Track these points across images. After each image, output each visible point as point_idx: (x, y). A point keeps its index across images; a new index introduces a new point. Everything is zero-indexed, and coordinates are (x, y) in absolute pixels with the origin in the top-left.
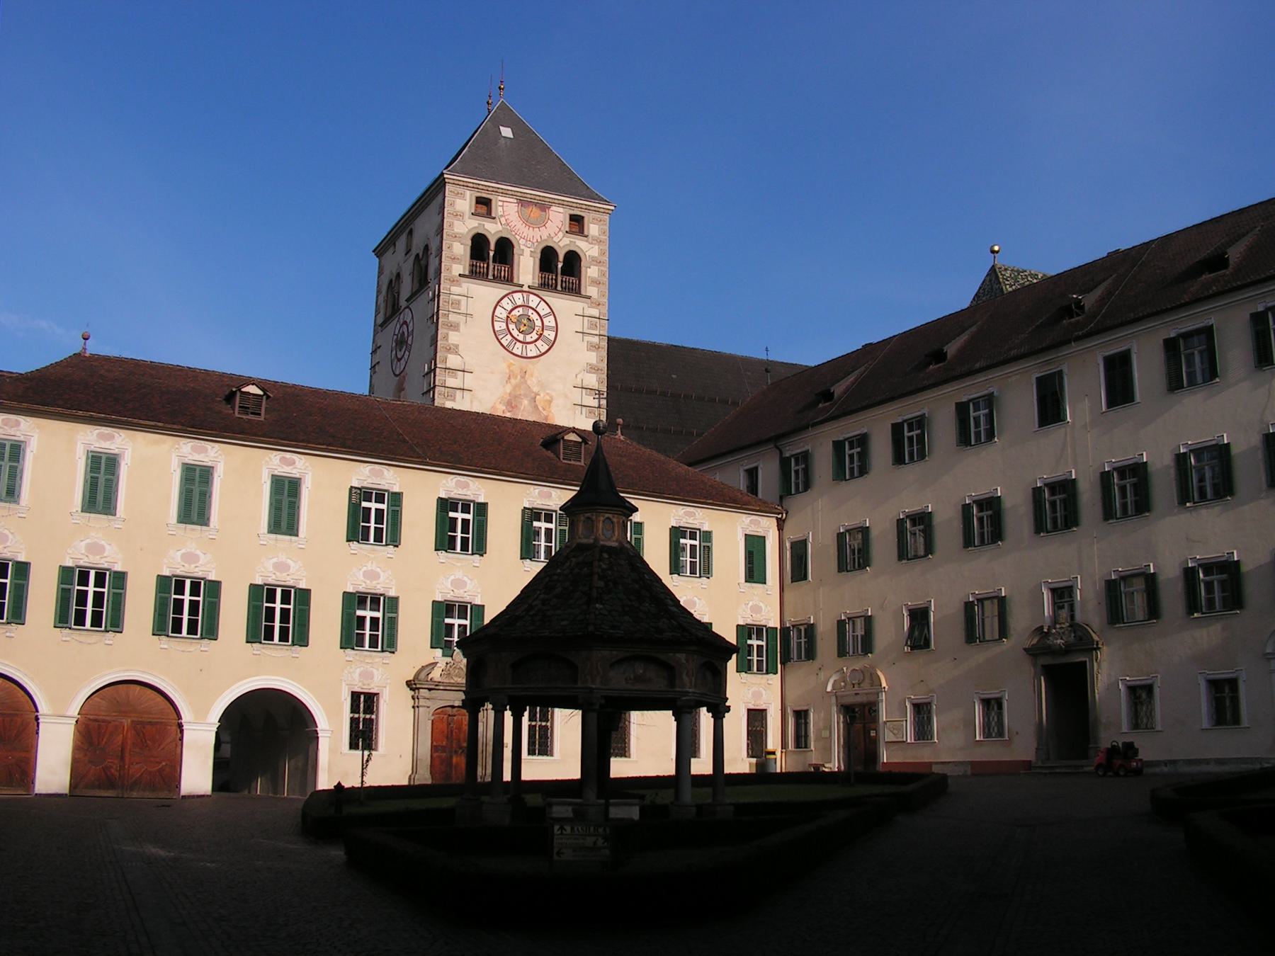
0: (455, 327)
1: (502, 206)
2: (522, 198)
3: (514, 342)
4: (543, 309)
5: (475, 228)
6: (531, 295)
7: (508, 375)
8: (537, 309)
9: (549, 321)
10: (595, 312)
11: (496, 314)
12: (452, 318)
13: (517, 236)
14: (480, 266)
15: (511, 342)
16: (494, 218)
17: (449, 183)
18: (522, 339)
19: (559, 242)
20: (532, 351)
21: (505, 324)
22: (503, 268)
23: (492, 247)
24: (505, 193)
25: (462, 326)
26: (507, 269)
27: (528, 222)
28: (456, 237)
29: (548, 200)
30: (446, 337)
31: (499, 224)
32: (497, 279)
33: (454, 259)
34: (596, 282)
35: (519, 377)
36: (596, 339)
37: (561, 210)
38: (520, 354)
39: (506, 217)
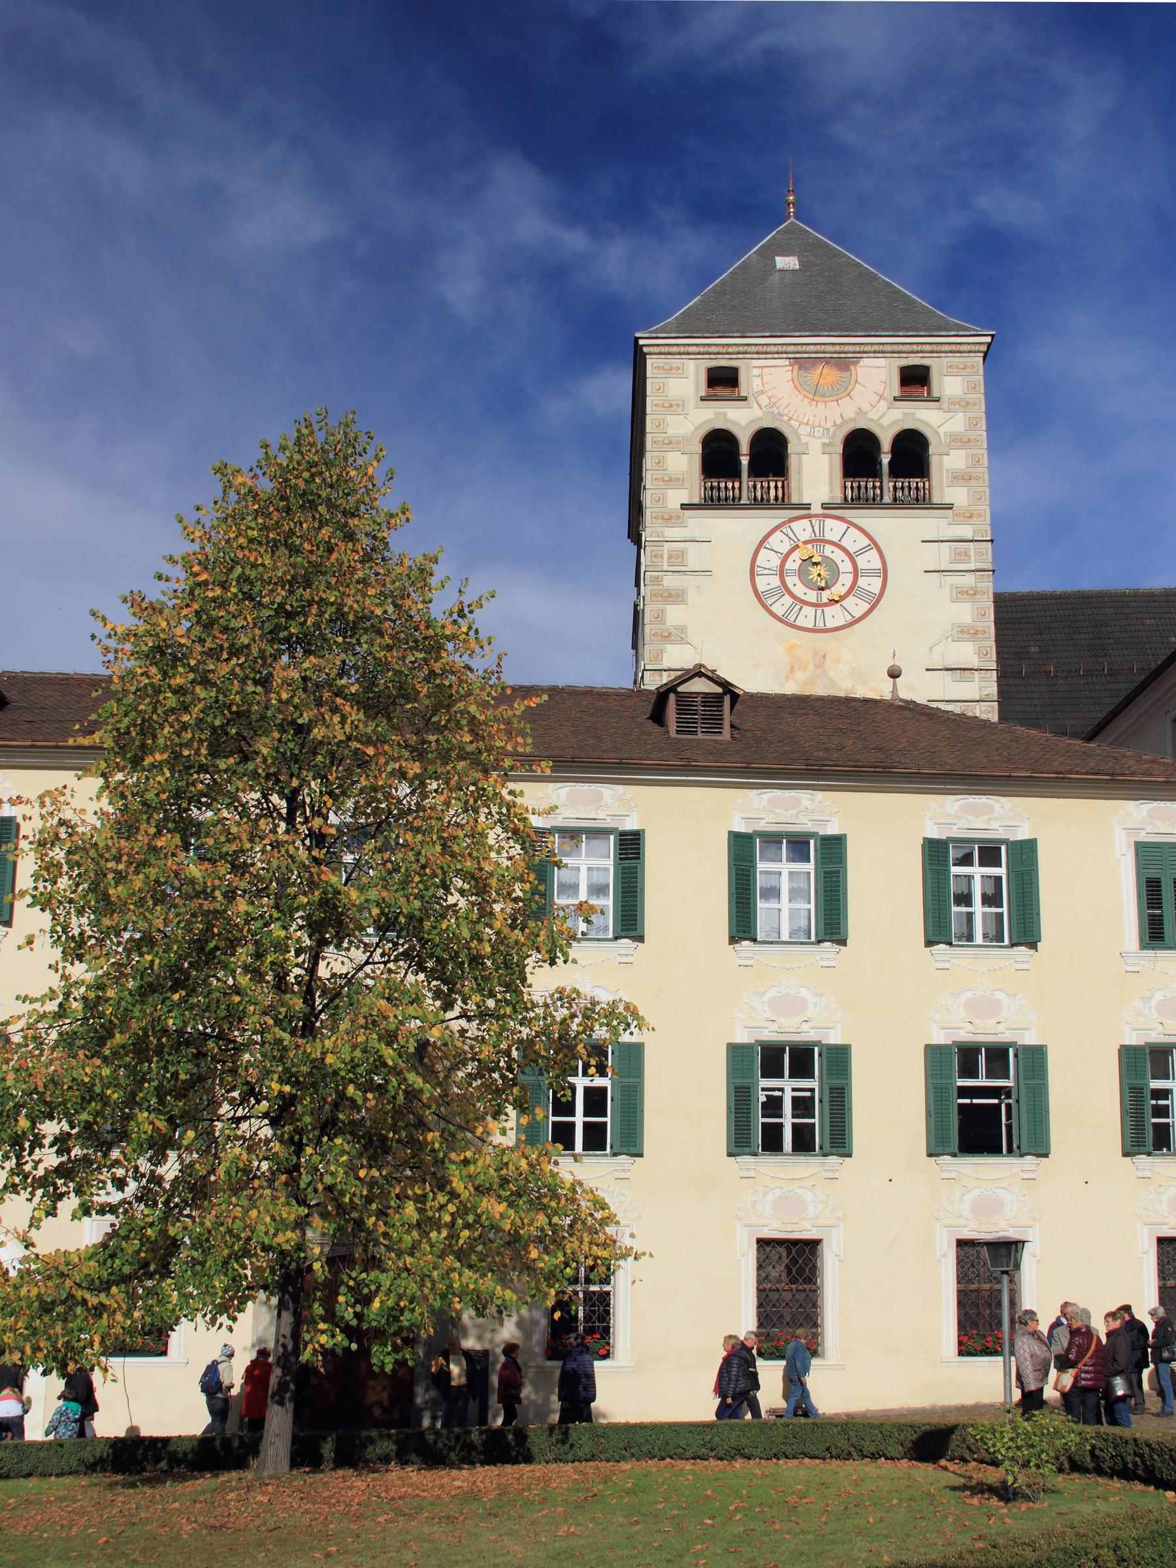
0: (677, 597)
1: (761, 376)
2: (798, 356)
3: (798, 607)
4: (854, 540)
5: (707, 421)
6: (828, 521)
7: (788, 667)
8: (843, 543)
9: (868, 561)
10: (966, 531)
11: (758, 563)
12: (670, 581)
13: (792, 422)
14: (726, 488)
15: (790, 610)
16: (745, 399)
17: (650, 354)
18: (814, 601)
19: (880, 418)
20: (835, 616)
21: (777, 578)
22: (772, 484)
23: (744, 448)
24: (763, 353)
25: (691, 596)
26: (780, 484)
27: (816, 394)
28: (670, 443)
29: (851, 348)
30: (660, 617)
31: (755, 405)
32: (760, 504)
33: (671, 481)
34: (961, 478)
35: (811, 667)
36: (969, 580)
37: (882, 362)
38: (811, 626)
39: (770, 394)
